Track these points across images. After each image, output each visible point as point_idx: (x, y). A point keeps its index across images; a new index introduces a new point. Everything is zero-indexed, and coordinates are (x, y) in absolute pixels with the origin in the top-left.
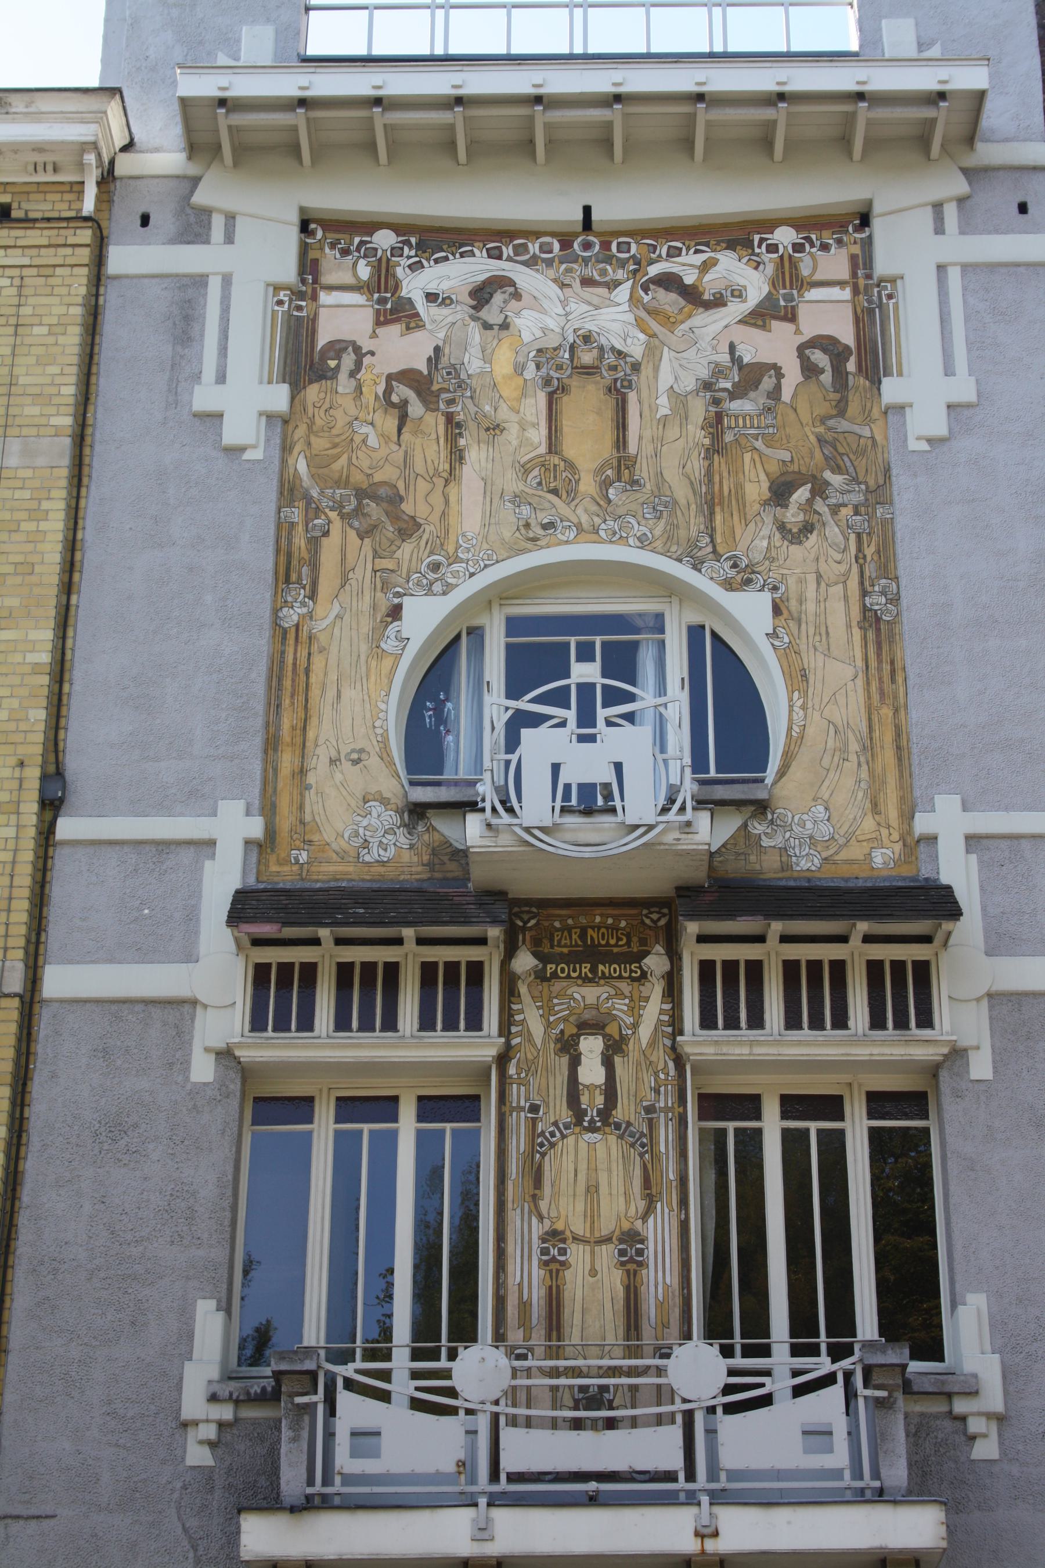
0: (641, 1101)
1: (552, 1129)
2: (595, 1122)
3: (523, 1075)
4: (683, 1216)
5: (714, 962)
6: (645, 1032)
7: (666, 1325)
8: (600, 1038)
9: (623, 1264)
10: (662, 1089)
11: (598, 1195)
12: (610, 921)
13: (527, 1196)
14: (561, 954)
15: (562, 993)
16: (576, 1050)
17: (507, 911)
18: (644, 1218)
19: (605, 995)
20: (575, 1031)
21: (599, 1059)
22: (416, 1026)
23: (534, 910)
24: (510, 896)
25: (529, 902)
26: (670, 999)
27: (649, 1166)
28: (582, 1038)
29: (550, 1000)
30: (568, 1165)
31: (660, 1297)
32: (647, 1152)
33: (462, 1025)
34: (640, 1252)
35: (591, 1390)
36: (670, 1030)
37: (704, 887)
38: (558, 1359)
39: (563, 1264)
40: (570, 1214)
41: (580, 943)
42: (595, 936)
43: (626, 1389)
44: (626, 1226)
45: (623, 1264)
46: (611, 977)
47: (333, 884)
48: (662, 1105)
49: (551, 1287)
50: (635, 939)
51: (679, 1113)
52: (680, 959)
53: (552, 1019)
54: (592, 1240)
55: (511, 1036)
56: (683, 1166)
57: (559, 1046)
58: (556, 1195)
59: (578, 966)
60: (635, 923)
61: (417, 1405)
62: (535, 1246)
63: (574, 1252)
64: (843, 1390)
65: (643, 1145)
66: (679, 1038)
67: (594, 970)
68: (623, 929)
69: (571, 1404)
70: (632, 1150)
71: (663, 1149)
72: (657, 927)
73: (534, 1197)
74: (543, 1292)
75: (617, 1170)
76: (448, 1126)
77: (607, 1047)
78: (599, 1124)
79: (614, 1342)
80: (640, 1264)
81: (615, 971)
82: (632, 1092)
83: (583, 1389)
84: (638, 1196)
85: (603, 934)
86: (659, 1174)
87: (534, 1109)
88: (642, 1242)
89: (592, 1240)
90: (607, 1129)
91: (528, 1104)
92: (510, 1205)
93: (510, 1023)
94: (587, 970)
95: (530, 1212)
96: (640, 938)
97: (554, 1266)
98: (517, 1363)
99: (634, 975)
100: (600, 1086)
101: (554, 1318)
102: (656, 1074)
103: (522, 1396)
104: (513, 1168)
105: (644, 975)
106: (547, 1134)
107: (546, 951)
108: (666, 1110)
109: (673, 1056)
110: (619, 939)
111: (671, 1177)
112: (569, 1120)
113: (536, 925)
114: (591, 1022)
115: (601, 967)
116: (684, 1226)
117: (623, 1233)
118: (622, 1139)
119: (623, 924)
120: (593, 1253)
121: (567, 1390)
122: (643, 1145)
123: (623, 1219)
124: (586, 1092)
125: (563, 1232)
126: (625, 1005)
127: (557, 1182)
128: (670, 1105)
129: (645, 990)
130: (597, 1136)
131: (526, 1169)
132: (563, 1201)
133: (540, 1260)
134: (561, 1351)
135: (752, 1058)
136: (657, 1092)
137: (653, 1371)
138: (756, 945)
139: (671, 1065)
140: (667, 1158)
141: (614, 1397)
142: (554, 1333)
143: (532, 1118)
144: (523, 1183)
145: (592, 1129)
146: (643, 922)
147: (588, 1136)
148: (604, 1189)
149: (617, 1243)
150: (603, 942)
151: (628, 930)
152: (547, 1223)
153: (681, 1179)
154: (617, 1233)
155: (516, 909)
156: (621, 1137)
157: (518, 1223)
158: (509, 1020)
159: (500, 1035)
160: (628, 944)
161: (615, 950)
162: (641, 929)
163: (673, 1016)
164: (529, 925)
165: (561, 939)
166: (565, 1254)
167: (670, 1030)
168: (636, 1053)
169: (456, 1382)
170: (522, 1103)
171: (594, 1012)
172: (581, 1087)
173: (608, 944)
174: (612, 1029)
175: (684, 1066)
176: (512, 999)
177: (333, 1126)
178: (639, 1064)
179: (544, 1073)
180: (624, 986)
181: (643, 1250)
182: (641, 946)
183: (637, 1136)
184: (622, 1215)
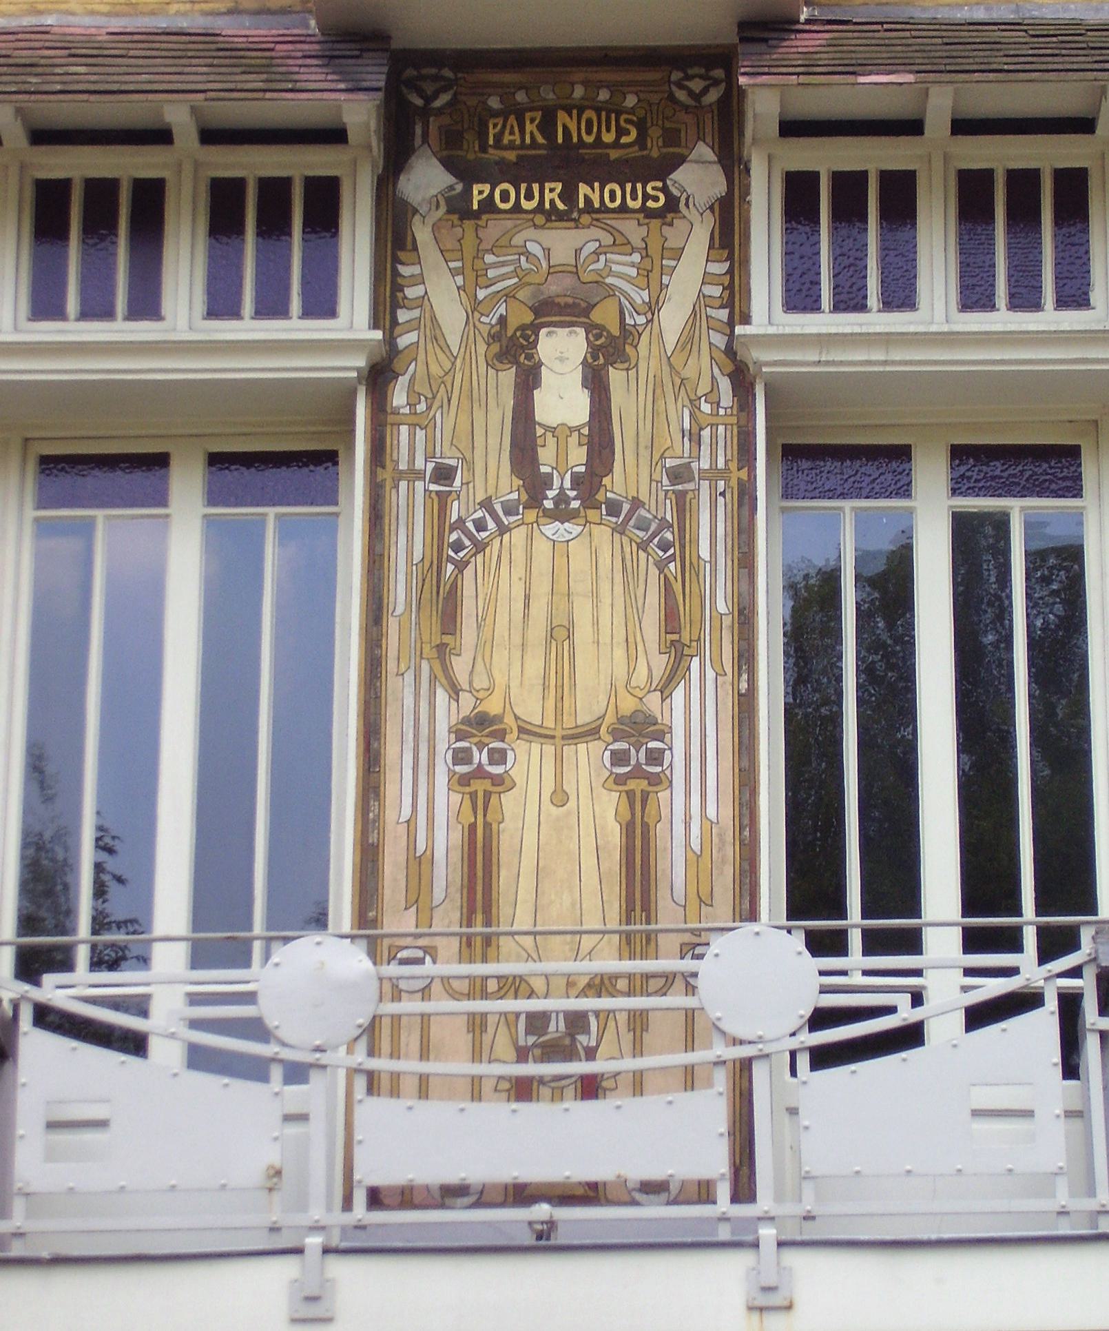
0: (662, 457)
1: (479, 514)
2: (567, 501)
3: (421, 407)
4: (744, 686)
5: (815, 176)
6: (673, 319)
7: (705, 901)
8: (581, 332)
9: (620, 780)
10: (706, 433)
11: (572, 647)
12: (604, 95)
13: (427, 649)
14: (501, 163)
15: (503, 242)
16: (529, 357)
17: (385, 69)
18: (665, 689)
19: (592, 246)
20: (528, 317)
21: (578, 376)
22: (200, 306)
23: (447, 73)
24: (395, 44)
25: (435, 58)
26: (725, 253)
27: (677, 587)
28: (543, 331)
29: (478, 255)
30: (510, 586)
31: (697, 848)
32: (672, 558)
33: (296, 304)
34: (655, 757)
35: (552, 1028)
36: (723, 314)
37: (798, 22)
38: (485, 960)
39: (498, 781)
40: (514, 684)
41: (540, 140)
42: (573, 127)
43: (622, 1018)
44: (628, 705)
45: (620, 780)
46: (604, 209)
47: (27, 21)
48: (705, 464)
49: (472, 828)
50: (655, 133)
51: (739, 480)
52: (748, 171)
53: (481, 294)
54: (558, 733)
55: (398, 330)
56: (745, 587)
57: (495, 348)
58: (485, 646)
59: (536, 187)
60: (655, 98)
61: (199, 1058)
62: (442, 746)
63: (522, 757)
64: (1055, 1020)
65: (665, 547)
66: (739, 330)
67: (569, 195)
68: (632, 111)
69: (512, 1055)
70: (642, 555)
71: (705, 553)
72: (700, 107)
73: (441, 649)
74: (457, 836)
75: (611, 594)
76: (271, 512)
77: (594, 351)
78: (575, 504)
79: (601, 927)
80: (655, 780)
81: (613, 199)
82: (645, 440)
83: (537, 1022)
84: (653, 646)
85: (589, 123)
86: (696, 601)
87: (444, 474)
88: (660, 736)
89: (558, 733)
90: (592, 514)
91: (430, 466)
92: (391, 665)
93: (395, 306)
94: (555, 195)
95: (433, 679)
96: (663, 128)
97: (480, 786)
98: (393, 970)
99: (650, 204)
100: (578, 429)
101: (479, 888)
102: (694, 404)
103: (411, 1040)
104: (399, 593)
105: (672, 205)
106: (470, 525)
107: (471, 156)
108: (713, 474)
109: (730, 367)
110: (621, 132)
111: (722, 607)
112: (515, 496)
113: (452, 103)
114: (562, 301)
115: (583, 189)
116: (746, 705)
117: (620, 720)
118: (622, 533)
119: (631, 101)
120: (559, 759)
121: (503, 1029)
122: (665, 547)
123: (622, 692)
124: (551, 441)
125: (499, 719)
126: (633, 265)
127: (489, 620)
128: (721, 464)
129: (674, 236)
130: (573, 528)
131: (426, 595)
132: (499, 659)
133: (452, 776)
134: (492, 951)
135: (888, 369)
136: (696, 439)
137: (679, 984)
138: (903, 140)
139: (725, 385)
140: (714, 571)
141: (598, 1046)
142: (479, 917)
143: (437, 493)
144: (418, 624)
145: (561, 513)
146: (672, 98)
147: (552, 529)
148: (583, 633)
149: (609, 739)
150: (589, 139)
151: (641, 113)
152: (467, 701)
153: (740, 612)
154: (610, 719)
155: (410, 72)
156: (620, 530)
157: (409, 701)
158: (393, 296)
159: (375, 325)
160: (641, 141)
161: (614, 154)
162: (669, 112)
163: (730, 287)
164: (437, 104)
165: (502, 133)
166: (503, 761)
167: (723, 314)
168: (654, 363)
169: (268, 1010)
170: (419, 464)
171: (568, 281)
172: (539, 431)
173: (598, 142)
174: (605, 315)
175: (752, 385)
176: (399, 253)
177: (31, 513)
178: (658, 385)
179: (465, 403)
180: (632, 229)
181: (662, 751)
182: (664, 146)
183: (653, 527)
184: (620, 684)
